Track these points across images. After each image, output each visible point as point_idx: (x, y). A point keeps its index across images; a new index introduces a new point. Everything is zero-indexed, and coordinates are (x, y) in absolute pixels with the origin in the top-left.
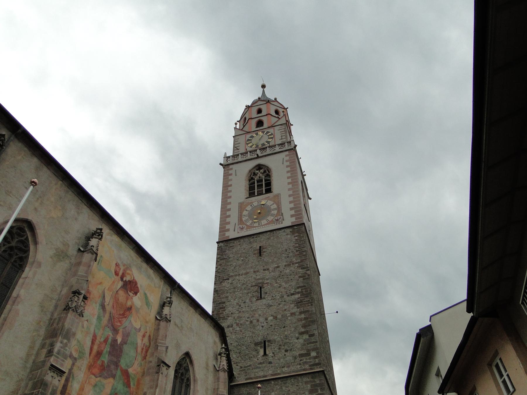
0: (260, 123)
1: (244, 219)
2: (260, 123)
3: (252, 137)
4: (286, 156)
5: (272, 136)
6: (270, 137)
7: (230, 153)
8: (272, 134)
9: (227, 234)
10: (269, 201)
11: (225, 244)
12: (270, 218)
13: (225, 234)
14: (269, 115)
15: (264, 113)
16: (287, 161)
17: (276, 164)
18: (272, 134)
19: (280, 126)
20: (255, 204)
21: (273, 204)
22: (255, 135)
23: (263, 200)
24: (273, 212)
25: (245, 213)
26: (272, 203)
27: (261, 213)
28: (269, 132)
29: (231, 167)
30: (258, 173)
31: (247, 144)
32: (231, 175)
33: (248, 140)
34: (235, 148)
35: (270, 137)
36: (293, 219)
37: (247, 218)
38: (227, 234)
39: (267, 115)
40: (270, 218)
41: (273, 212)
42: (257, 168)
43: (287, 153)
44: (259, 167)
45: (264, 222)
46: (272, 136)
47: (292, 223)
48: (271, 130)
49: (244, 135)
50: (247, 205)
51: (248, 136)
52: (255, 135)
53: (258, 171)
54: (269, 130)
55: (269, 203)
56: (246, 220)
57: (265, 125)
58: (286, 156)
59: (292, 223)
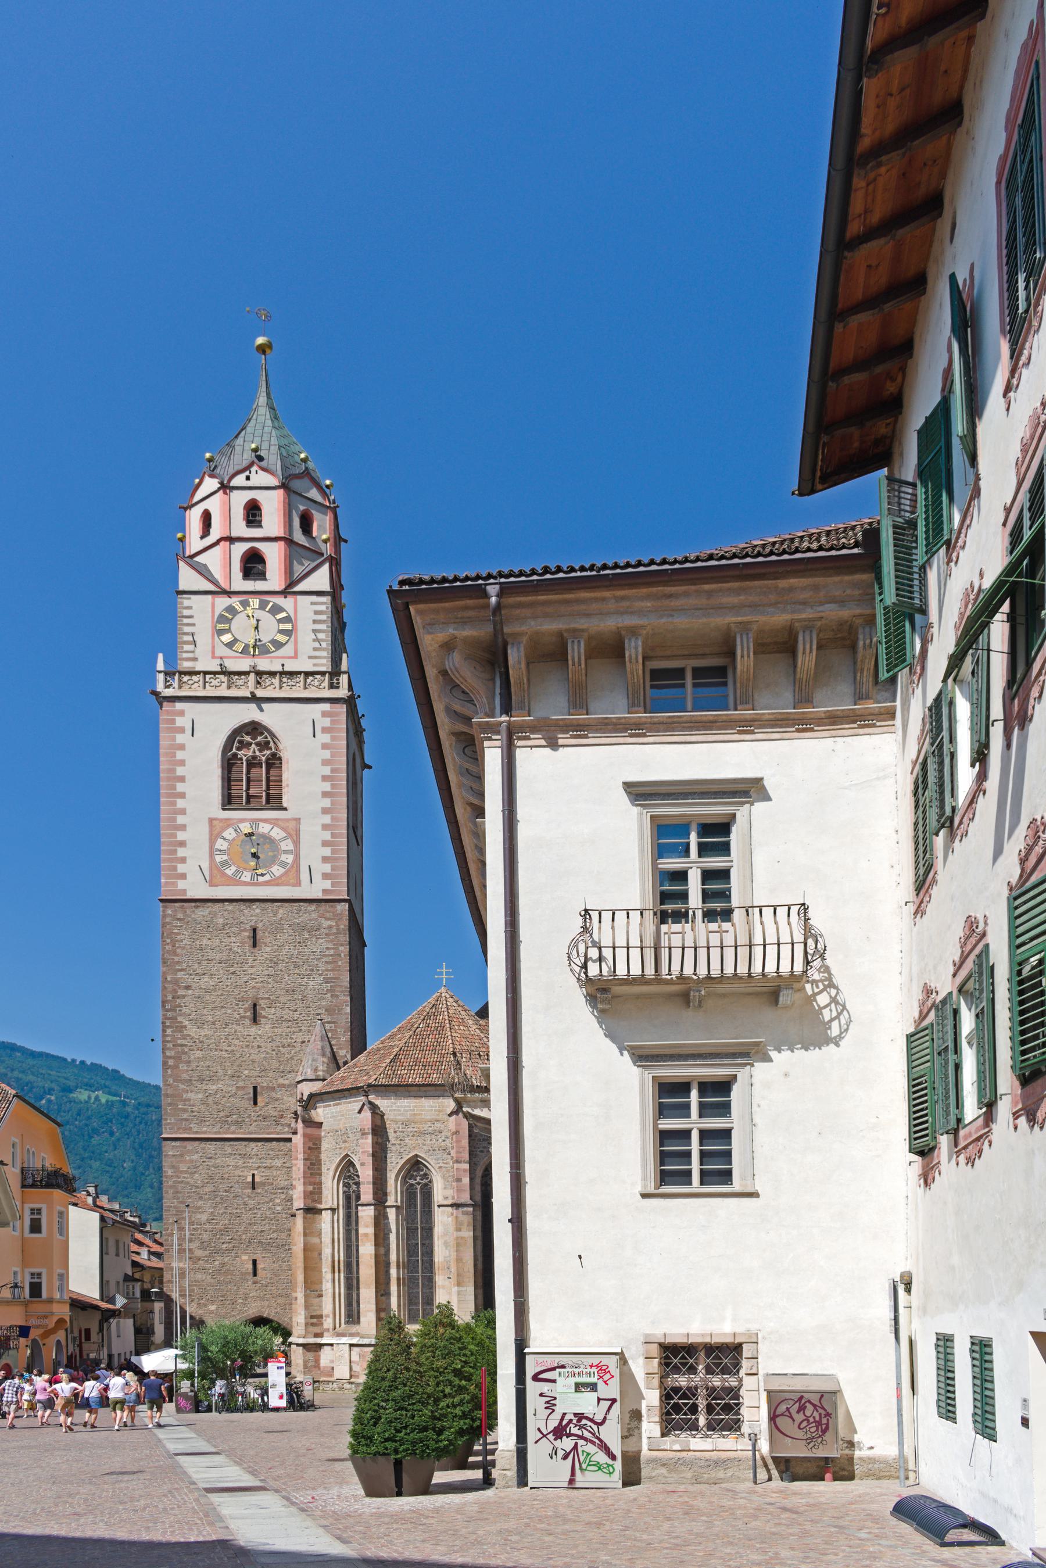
1: (218, 859)
3: (231, 609)
12: (277, 870)
20: (246, 828)
21: (285, 839)
23: (263, 821)
24: (283, 857)
25: (221, 844)
26: (283, 834)
28: (282, 610)
31: (221, 632)
33: (222, 619)
37: (225, 857)
40: (277, 870)
44: (254, 728)
50: (228, 826)
51: (223, 602)
53: (248, 738)
55: (277, 833)
56: (224, 863)
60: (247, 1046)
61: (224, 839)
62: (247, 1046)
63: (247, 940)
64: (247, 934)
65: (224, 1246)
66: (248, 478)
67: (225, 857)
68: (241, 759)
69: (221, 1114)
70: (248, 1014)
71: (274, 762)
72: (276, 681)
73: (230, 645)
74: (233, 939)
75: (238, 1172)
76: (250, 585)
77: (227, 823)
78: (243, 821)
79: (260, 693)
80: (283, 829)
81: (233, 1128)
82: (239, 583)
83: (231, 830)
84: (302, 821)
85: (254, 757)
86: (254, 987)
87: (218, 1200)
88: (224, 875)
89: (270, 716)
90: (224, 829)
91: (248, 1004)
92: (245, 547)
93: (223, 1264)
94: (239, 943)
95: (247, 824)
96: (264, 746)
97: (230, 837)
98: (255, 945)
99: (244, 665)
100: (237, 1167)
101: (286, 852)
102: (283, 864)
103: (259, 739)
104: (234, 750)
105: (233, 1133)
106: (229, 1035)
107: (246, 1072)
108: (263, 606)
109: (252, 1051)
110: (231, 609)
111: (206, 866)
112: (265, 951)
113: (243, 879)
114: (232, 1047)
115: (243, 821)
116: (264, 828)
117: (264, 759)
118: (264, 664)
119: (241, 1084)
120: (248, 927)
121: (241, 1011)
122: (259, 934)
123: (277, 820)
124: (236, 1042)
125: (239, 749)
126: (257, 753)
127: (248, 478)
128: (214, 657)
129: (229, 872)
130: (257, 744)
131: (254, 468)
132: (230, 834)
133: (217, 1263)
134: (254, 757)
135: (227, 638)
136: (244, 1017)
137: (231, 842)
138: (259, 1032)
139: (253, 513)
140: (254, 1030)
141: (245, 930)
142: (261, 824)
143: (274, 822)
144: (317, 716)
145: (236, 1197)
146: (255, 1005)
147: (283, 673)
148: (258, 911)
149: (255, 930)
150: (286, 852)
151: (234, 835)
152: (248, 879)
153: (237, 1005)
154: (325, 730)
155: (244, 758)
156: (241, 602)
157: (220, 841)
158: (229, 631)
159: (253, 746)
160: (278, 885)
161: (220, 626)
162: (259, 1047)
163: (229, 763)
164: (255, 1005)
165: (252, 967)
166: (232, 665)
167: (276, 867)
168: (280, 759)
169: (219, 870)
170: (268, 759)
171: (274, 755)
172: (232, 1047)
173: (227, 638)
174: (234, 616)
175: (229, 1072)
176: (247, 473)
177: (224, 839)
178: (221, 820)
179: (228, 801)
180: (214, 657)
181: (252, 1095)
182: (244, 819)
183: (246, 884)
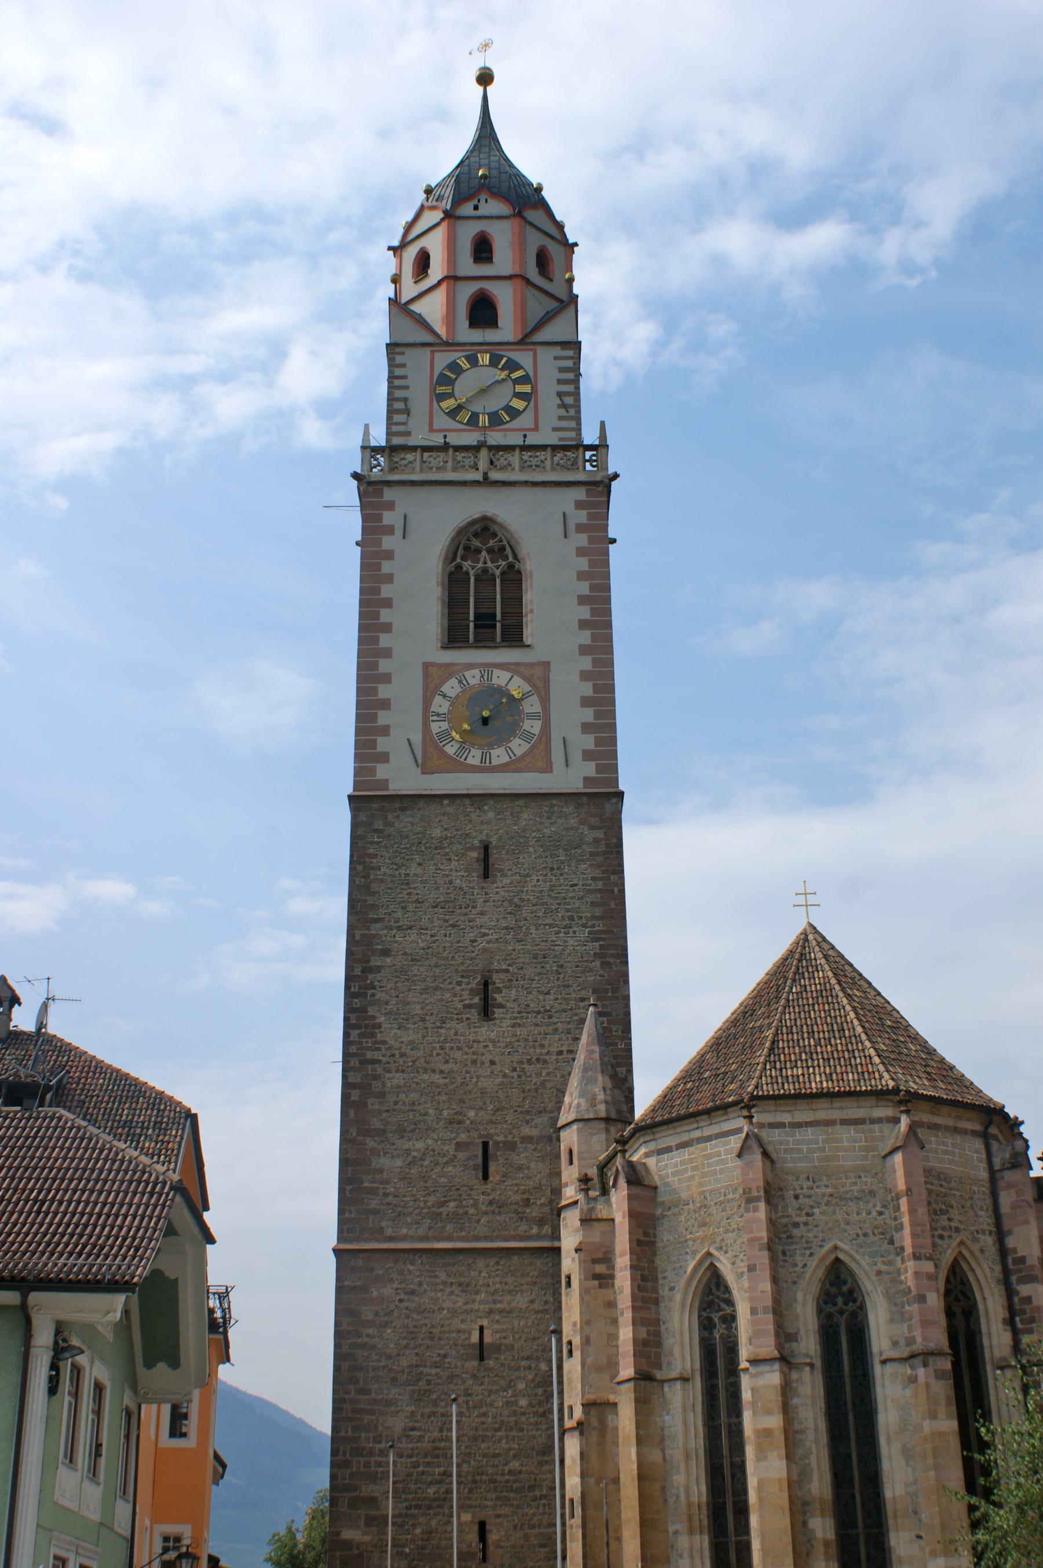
0: (483, 312)
1: (435, 728)
2: (483, 312)
3: (454, 367)
4: (579, 505)
5: (527, 389)
6: (519, 388)
7: (379, 437)
8: (525, 380)
9: (382, 771)
10: (517, 681)
11: (372, 809)
13: (372, 771)
14: (518, 281)
15: (504, 260)
16: (580, 528)
17: (536, 523)
18: (525, 380)
19: (558, 351)
20: (473, 677)
22: (464, 364)
25: (439, 705)
27: (491, 717)
29: (388, 494)
30: (478, 551)
31: (441, 397)
32: (390, 530)
33: (443, 380)
34: (397, 406)
35: (519, 388)
36: (590, 769)
37: (445, 725)
38: (382, 771)
39: (510, 277)
40: (519, 746)
41: (527, 725)
42: (477, 527)
43: (580, 494)
45: (499, 756)
46: (527, 389)
47: (587, 780)
48: (523, 358)
49: (428, 350)
51: (443, 359)
52: (464, 364)
53: (476, 543)
54: (517, 356)
55: (517, 687)
56: (445, 735)
57: (507, 329)
58: (579, 505)
59: (587, 780)
60: (474, 1062)
61: (444, 696)
62: (474, 1062)
63: (476, 866)
64: (475, 855)
65: (431, 1491)
66: (476, 208)
67: (445, 725)
68: (467, 573)
69: (432, 1199)
70: (476, 1000)
71: (514, 578)
72: (515, 458)
73: (453, 413)
74: (454, 864)
75: (456, 1324)
76: (477, 335)
77: (449, 670)
78: (471, 666)
79: (495, 476)
80: (528, 679)
81: (449, 1228)
82: (466, 334)
83: (453, 681)
84: (552, 666)
85: (485, 571)
86: (484, 950)
87: (422, 1384)
88: (443, 754)
89: (511, 511)
90: (444, 681)
91: (475, 983)
92: (472, 288)
93: (429, 1533)
94: (460, 873)
95: (476, 672)
96: (498, 552)
97: (452, 693)
98: (486, 875)
99: (470, 438)
100: (454, 1312)
101: (532, 716)
102: (527, 736)
103: (491, 543)
104: (459, 560)
105: (450, 1239)
106: (445, 1041)
107: (471, 1114)
108: (494, 362)
109: (481, 1072)
110: (454, 367)
111: (417, 739)
112: (502, 884)
113: (470, 761)
114: (451, 1065)
115: (471, 666)
116: (500, 678)
117: (498, 572)
118: (496, 438)
119: (463, 1137)
120: (476, 843)
121: (465, 994)
122: (494, 854)
123: (517, 664)
124: (458, 1055)
125: (463, 558)
126: (489, 564)
127: (476, 208)
128: (431, 430)
129: (451, 750)
130: (490, 551)
131: (483, 197)
132: (451, 688)
133: (418, 1531)
134: (485, 571)
135: (449, 404)
136: (469, 1006)
137: (454, 702)
138: (493, 1035)
139: (483, 250)
140: (485, 1031)
141: (473, 848)
142: (496, 672)
143: (513, 668)
144: (569, 508)
145: (451, 1378)
146: (486, 984)
147: (524, 448)
148: (491, 815)
149: (486, 848)
150: (532, 716)
151: (458, 689)
152: (476, 761)
153: (459, 983)
154: (580, 528)
155: (472, 572)
156: (467, 358)
157: (438, 699)
158: (451, 395)
159: (484, 553)
160: (519, 771)
161: (441, 389)
162: (492, 1063)
163: (455, 581)
164: (486, 984)
165: (482, 913)
166: (454, 440)
167: (517, 741)
168: (519, 572)
169: (436, 746)
170: (503, 573)
171: (511, 566)
172: (451, 1065)
173: (449, 404)
174: (458, 375)
175: (445, 1113)
176: (475, 202)
177: (444, 696)
178: (440, 666)
179: (454, 636)
180: (431, 430)
181: (480, 1160)
182: (475, 661)
183: (474, 769)
